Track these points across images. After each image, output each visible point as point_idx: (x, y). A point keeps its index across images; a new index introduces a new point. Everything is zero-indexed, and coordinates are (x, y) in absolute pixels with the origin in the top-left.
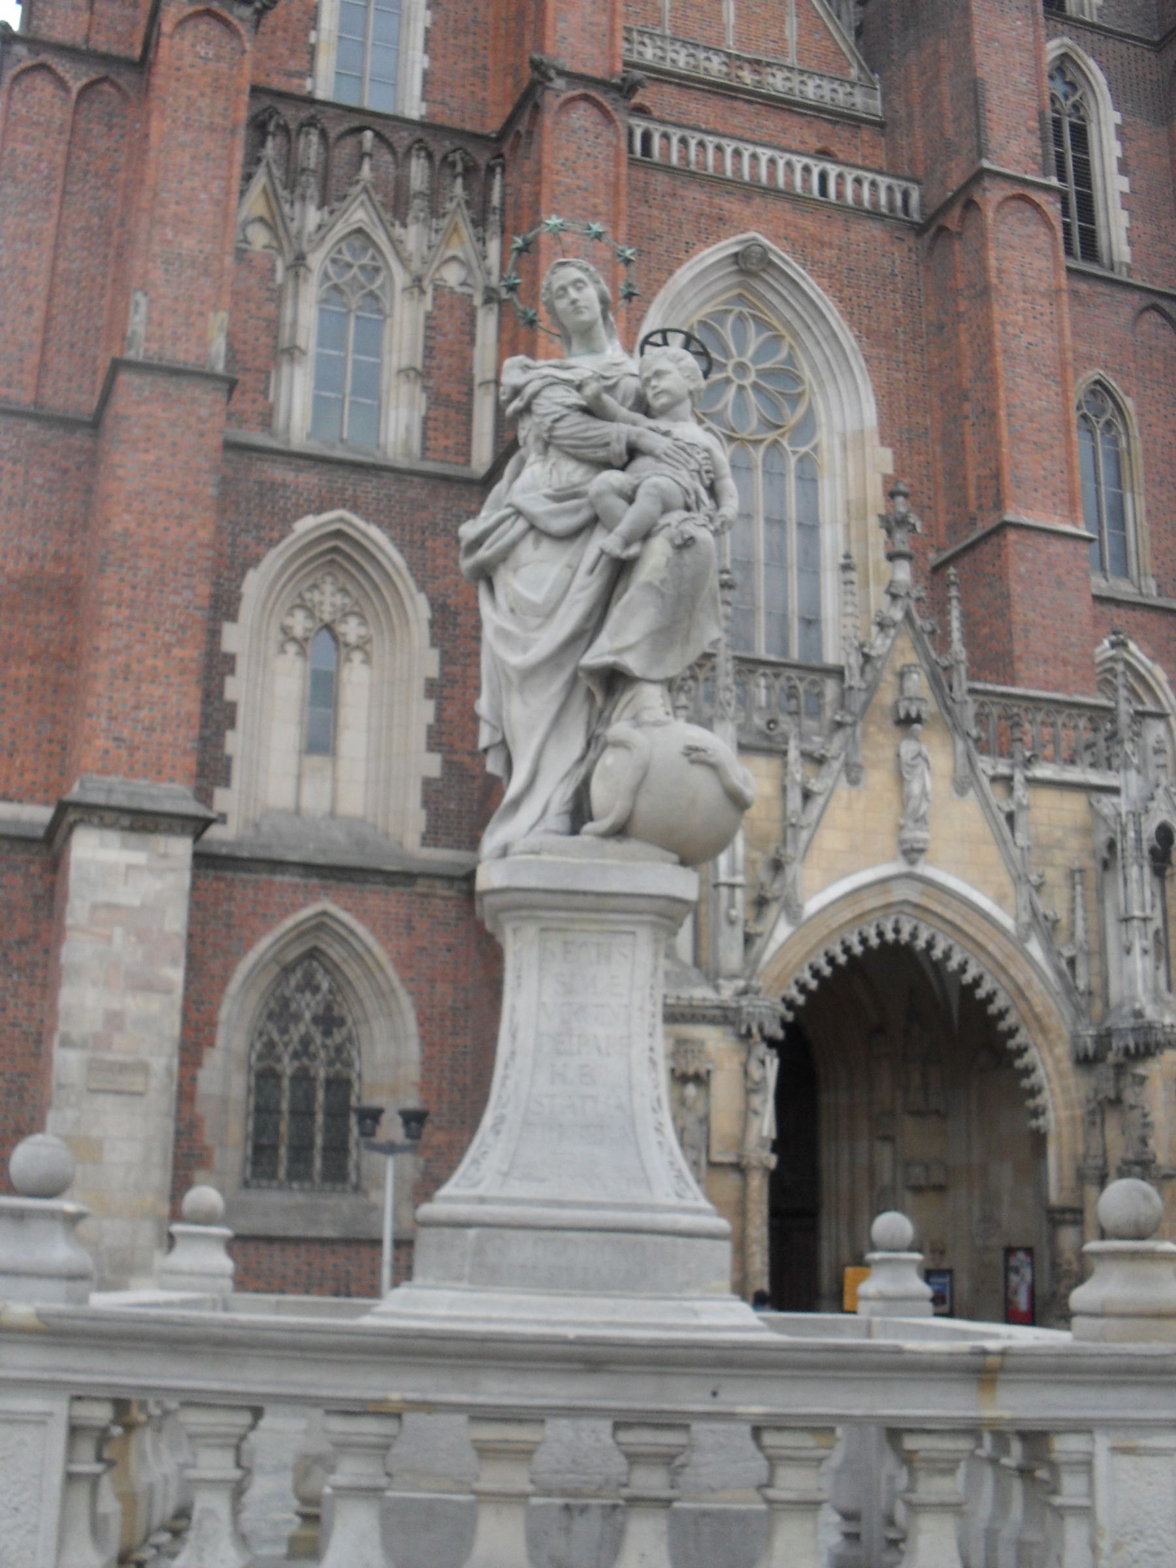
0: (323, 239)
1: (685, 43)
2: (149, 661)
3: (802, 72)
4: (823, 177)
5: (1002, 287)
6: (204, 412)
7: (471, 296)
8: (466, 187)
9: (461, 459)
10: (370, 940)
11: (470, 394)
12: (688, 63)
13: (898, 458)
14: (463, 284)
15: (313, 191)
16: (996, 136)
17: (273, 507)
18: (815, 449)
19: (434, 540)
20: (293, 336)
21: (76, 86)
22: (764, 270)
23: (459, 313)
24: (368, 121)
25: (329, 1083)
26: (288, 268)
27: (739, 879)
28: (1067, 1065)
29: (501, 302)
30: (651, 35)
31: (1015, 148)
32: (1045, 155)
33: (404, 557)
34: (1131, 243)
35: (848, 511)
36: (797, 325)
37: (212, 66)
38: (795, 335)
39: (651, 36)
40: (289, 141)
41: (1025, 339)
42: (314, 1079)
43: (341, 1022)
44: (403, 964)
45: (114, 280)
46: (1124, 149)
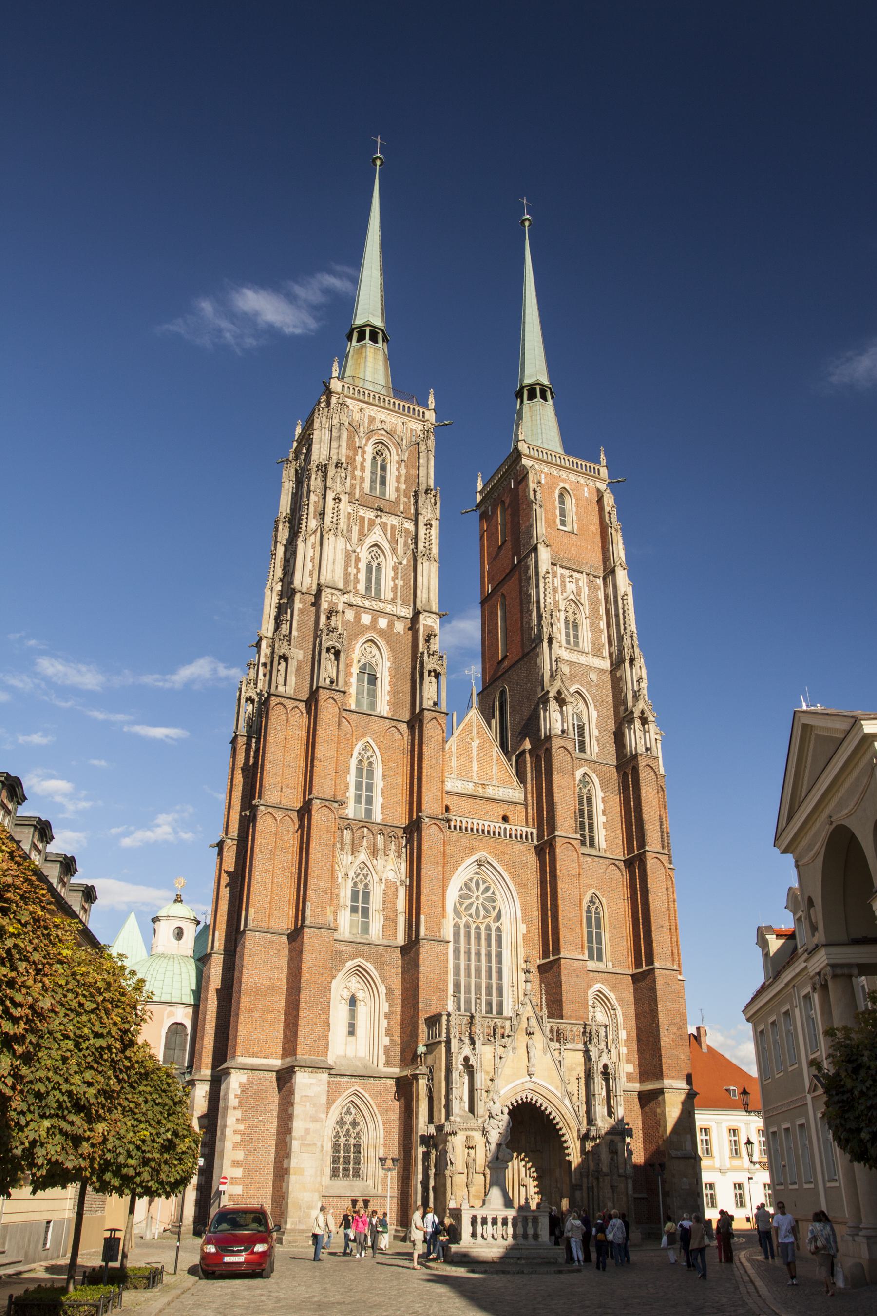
2: (314, 1020)
4: (505, 829)
5: (561, 876)
9: (394, 938)
11: (396, 916)
15: (350, 852)
23: (393, 888)
25: (354, 1145)
27: (483, 1087)
31: (566, 824)
32: (576, 826)
34: (606, 841)
41: (568, 892)
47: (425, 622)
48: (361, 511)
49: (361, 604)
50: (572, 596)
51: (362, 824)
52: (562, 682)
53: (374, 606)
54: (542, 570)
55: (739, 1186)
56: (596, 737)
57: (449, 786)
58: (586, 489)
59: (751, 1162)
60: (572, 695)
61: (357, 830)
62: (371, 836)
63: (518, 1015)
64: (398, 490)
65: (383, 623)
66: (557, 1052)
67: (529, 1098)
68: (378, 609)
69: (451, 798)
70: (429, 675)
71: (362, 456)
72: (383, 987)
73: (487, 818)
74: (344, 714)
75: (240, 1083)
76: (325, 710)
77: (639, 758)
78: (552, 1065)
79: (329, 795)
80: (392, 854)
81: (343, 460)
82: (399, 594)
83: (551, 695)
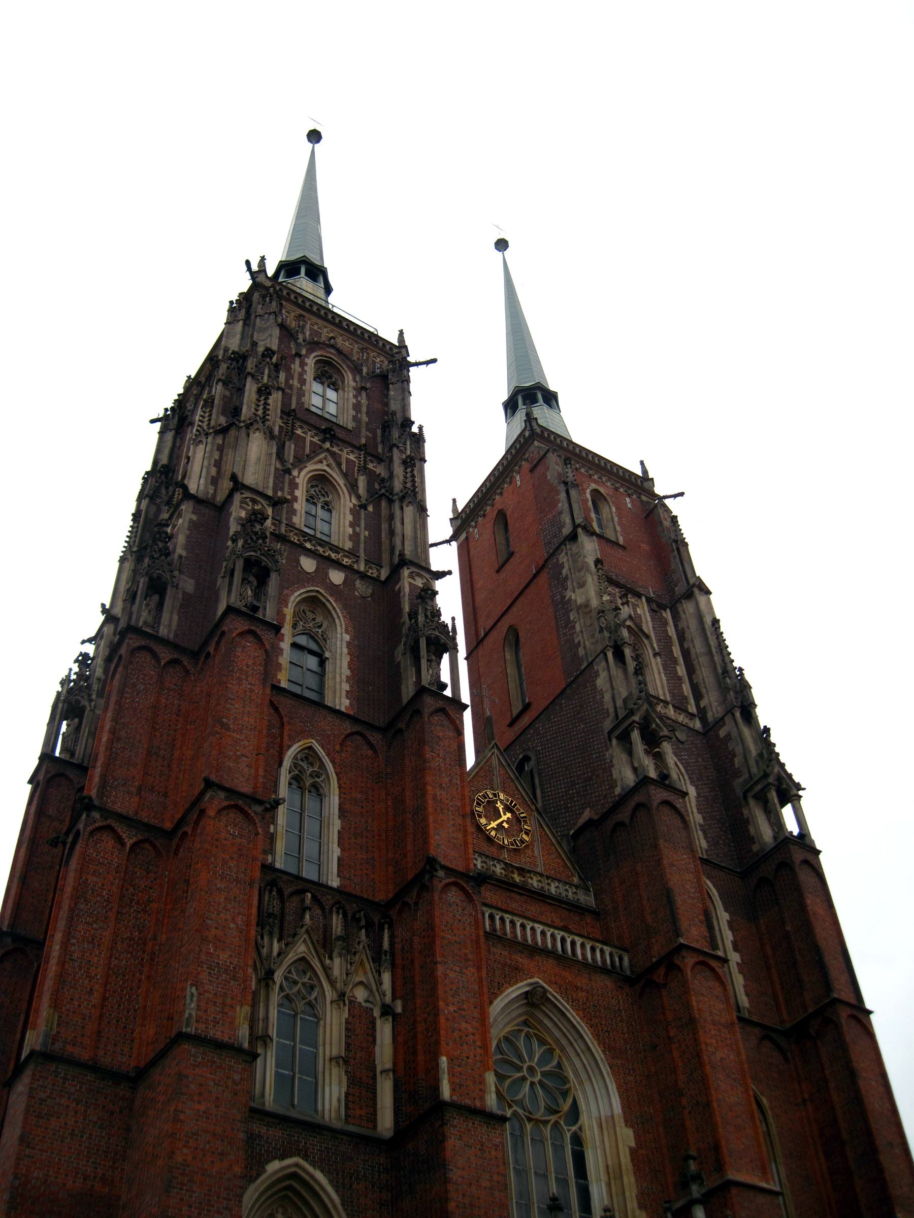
0: (281, 963)
1: (481, 854)
3: (548, 877)
7: (372, 1010)
8: (367, 936)
9: (371, 1126)
11: (374, 1078)
12: (483, 867)
13: (637, 1136)
14: (367, 1001)
15: (276, 930)
16: (684, 924)
17: (252, 1152)
18: (580, 1128)
19: (358, 1184)
20: (266, 1028)
21: (129, 843)
22: (542, 1004)
26: (259, 981)
29: (395, 1016)
33: (338, 1195)
34: (747, 995)
35: (608, 1173)
36: (564, 1042)
37: (238, 840)
38: (562, 1049)
45: (148, 977)
46: (734, 936)
56: (701, 825)
61: (291, 895)
64: (355, 418)
77: (791, 846)
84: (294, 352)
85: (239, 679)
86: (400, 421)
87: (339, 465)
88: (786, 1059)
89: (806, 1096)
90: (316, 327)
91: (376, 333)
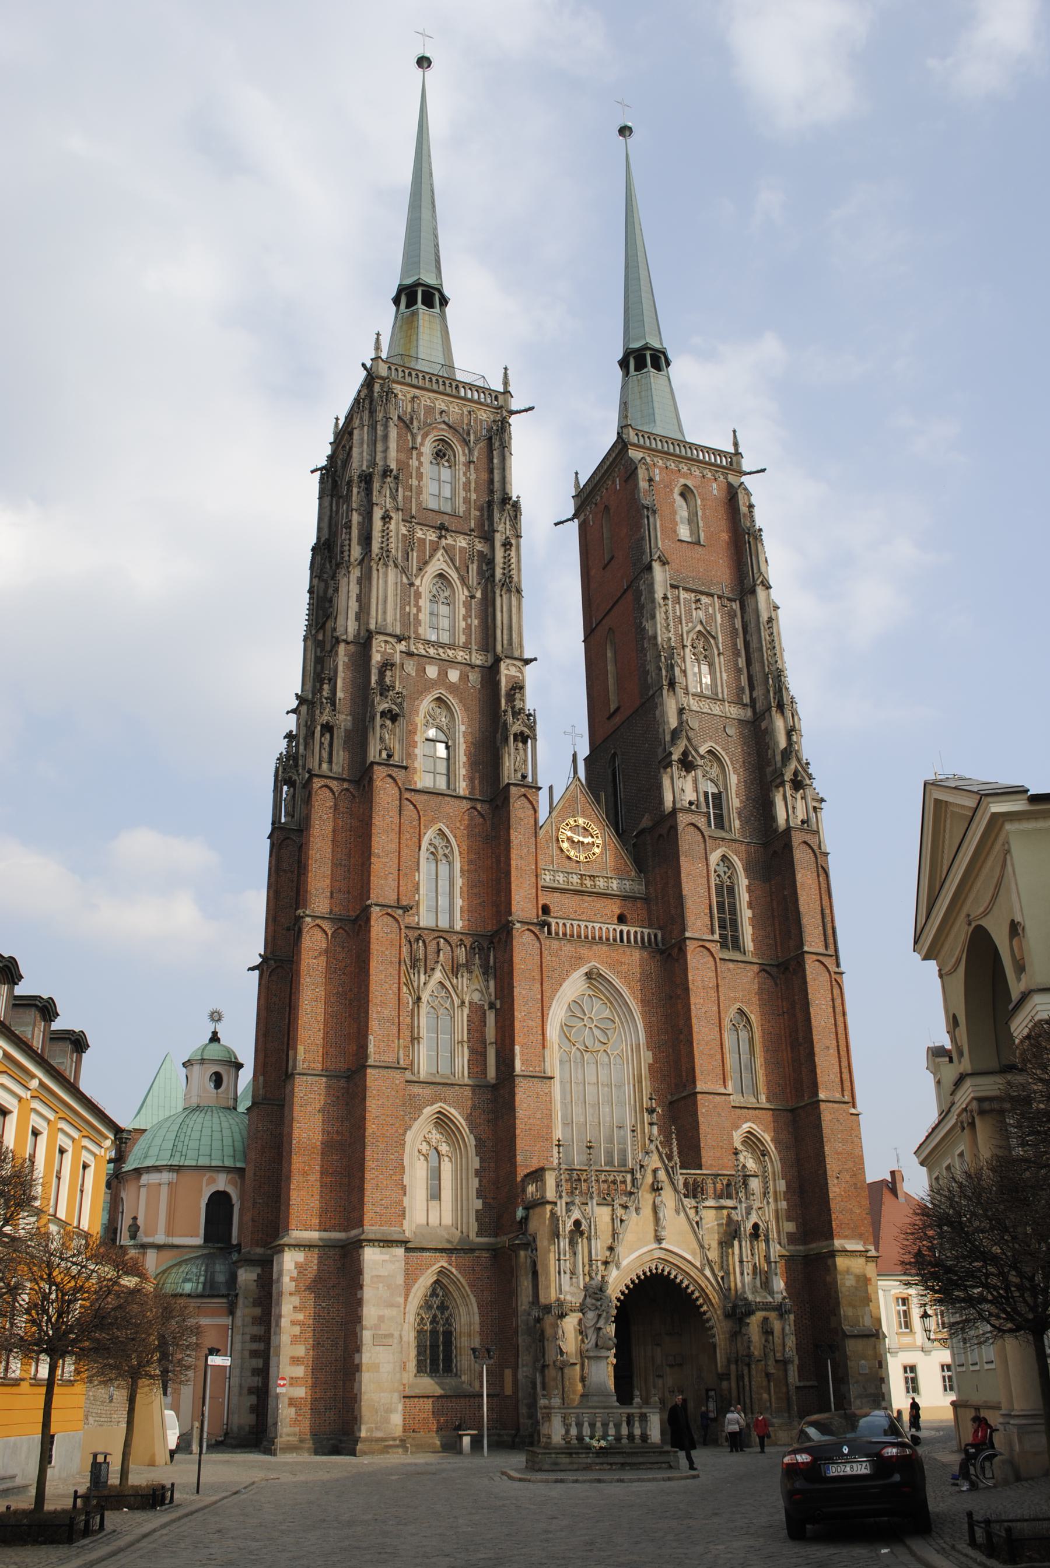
4: (621, 932)
6: (397, 1082)
9: (483, 1076)
10: (459, 1276)
13: (654, 1055)
21: (330, 933)
24: (441, 934)
25: (444, 1332)
26: (414, 1003)
27: (599, 1258)
28: (721, 1318)
29: (496, 1010)
30: (548, 870)
31: (699, 923)
34: (753, 941)
39: (548, 870)
40: (411, 946)
42: (438, 1332)
43: (448, 1308)
44: (472, 1285)
46: (750, 897)
47: (506, 672)
48: (420, 532)
49: (423, 652)
50: (699, 628)
51: (436, 934)
52: (689, 739)
53: (441, 654)
54: (659, 595)
55: (913, 1369)
57: (547, 878)
58: (715, 485)
59: (929, 1339)
60: (702, 757)
62: (449, 948)
63: (642, 1166)
64: (467, 501)
65: (454, 676)
66: (693, 1211)
67: (660, 1267)
68: (447, 658)
69: (550, 895)
70: (515, 740)
71: (418, 459)
72: (472, 1137)
73: (598, 918)
74: (407, 795)
75: (296, 1263)
76: (382, 792)
77: (793, 833)
78: (687, 1227)
79: (391, 898)
80: (477, 971)
81: (393, 466)
82: (473, 636)
83: (675, 757)
84: (410, 446)
85: (384, 816)
86: (497, 497)
87: (452, 561)
88: (776, 984)
89: (785, 1010)
90: (428, 403)
91: (480, 383)
